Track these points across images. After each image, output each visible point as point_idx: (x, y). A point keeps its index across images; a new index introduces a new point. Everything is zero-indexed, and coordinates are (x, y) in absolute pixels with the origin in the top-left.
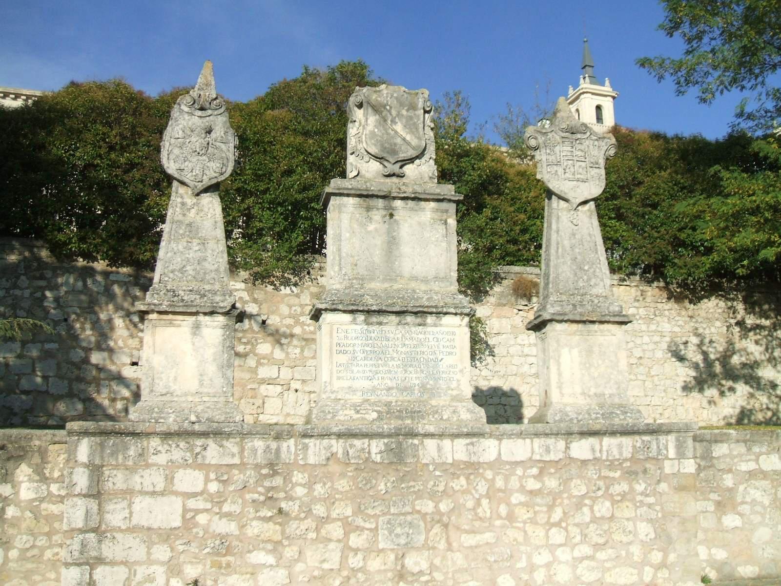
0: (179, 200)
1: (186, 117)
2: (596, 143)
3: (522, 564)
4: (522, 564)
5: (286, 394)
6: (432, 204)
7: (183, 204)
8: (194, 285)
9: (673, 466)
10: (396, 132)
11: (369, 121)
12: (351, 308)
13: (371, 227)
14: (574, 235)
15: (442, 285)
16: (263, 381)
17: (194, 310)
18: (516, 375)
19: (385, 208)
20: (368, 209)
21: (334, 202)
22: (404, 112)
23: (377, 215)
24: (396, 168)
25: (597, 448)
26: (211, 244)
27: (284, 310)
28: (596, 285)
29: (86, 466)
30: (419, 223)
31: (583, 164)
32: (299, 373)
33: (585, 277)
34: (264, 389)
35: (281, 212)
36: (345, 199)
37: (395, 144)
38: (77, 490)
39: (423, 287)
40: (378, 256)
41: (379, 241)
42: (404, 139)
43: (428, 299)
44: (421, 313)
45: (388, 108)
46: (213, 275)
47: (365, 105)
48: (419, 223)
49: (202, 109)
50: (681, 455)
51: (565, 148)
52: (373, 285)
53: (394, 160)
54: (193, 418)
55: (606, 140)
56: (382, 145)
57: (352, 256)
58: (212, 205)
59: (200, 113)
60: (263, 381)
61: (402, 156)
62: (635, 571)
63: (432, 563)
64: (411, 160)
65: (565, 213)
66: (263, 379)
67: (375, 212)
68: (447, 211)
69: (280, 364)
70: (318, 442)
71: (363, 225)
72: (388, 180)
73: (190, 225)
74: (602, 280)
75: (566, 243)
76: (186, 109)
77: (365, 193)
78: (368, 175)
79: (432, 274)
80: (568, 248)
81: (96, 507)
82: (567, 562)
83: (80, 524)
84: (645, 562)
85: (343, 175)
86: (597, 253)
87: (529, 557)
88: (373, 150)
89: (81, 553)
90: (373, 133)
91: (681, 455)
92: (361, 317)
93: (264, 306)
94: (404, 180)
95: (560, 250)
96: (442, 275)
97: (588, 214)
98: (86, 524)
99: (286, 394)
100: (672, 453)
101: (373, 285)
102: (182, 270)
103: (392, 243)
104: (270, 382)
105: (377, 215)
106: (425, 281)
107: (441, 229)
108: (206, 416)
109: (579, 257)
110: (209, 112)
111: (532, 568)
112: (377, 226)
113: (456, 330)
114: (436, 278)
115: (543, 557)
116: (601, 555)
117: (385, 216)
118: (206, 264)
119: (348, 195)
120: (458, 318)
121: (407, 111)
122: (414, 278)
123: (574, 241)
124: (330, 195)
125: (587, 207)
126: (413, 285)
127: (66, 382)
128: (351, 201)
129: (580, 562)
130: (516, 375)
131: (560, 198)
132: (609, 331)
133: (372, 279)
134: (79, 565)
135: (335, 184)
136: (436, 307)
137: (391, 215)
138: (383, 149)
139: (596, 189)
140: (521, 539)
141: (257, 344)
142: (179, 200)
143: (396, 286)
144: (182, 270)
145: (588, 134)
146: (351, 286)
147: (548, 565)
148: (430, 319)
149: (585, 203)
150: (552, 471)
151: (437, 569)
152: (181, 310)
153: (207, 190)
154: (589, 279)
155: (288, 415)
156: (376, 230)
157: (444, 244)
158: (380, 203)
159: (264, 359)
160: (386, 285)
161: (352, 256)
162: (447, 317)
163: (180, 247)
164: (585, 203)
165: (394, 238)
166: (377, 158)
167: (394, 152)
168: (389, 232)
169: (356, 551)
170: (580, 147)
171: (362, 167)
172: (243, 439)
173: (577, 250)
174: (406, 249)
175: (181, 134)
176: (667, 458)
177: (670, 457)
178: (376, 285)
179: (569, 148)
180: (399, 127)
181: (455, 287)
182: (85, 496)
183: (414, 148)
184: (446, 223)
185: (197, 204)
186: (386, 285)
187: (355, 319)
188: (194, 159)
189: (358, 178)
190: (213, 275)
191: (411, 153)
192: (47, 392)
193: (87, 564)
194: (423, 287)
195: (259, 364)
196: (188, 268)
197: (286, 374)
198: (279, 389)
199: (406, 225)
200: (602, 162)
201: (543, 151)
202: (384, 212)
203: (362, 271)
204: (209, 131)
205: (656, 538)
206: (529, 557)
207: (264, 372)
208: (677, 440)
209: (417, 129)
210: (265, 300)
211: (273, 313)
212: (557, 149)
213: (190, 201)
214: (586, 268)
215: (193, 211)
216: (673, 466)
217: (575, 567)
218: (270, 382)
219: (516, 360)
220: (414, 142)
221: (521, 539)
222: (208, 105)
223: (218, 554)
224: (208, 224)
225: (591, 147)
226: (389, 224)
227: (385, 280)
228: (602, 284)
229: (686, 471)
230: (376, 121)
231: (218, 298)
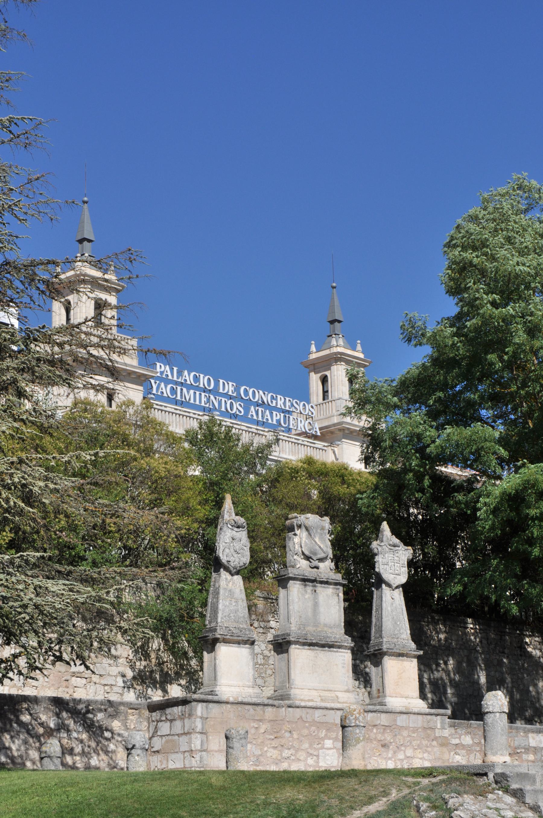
7: (226, 579)
13: (307, 596)
14: (392, 604)
20: (305, 585)
22: (319, 531)
26: (240, 603)
29: (201, 718)
38: (198, 730)
41: (310, 604)
42: (320, 547)
44: (330, 646)
46: (242, 619)
47: (303, 526)
59: (236, 529)
71: (302, 595)
72: (313, 570)
73: (230, 591)
75: (389, 608)
81: (205, 739)
88: (307, 553)
98: (201, 748)
100: (439, 726)
102: (229, 616)
103: (316, 605)
106: (331, 628)
122: (325, 625)
138: (311, 552)
139: (403, 579)
154: (400, 630)
156: (309, 598)
157: (338, 607)
165: (316, 603)
181: (343, 631)
184: (338, 596)
190: (242, 619)
196: (232, 615)
200: (406, 563)
208: (442, 719)
212: (387, 555)
215: (231, 583)
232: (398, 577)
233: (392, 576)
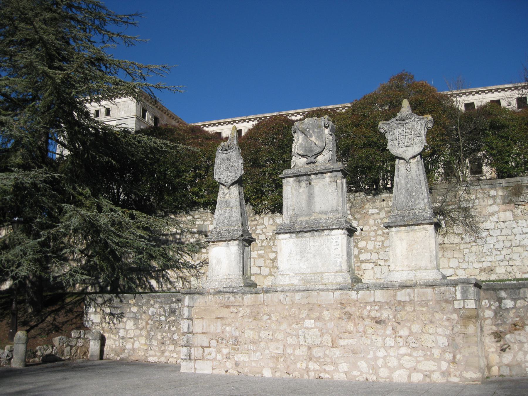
0: (222, 191)
1: (221, 155)
2: (419, 122)
3: (371, 356)
4: (371, 356)
5: (375, 268)
6: (329, 174)
7: (224, 193)
8: (227, 228)
9: (459, 304)
10: (312, 141)
11: (300, 139)
12: (287, 231)
13: (301, 190)
14: (407, 177)
15: (334, 214)
16: (362, 262)
17: (224, 239)
18: (518, 246)
19: (307, 180)
20: (299, 182)
21: (284, 181)
22: (316, 130)
23: (304, 184)
24: (312, 159)
25: (412, 295)
26: (235, 209)
27: (371, 222)
28: (419, 203)
29: (188, 307)
30: (323, 185)
31: (410, 136)
32: (382, 256)
33: (413, 200)
34: (364, 266)
35: (262, 191)
36: (289, 179)
37: (311, 147)
38: (185, 317)
39: (325, 217)
40: (304, 204)
41: (304, 197)
42: (315, 144)
43: (325, 223)
45: (308, 130)
46: (235, 223)
48: (323, 185)
49: (226, 150)
50: (465, 298)
51: (400, 130)
52: (301, 219)
53: (311, 155)
54: (225, 286)
55: (424, 120)
56: (305, 149)
57: (292, 206)
58: (235, 191)
59: (225, 152)
60: (362, 262)
61: (315, 152)
62: (436, 364)
63: (325, 353)
64: (320, 153)
65: (402, 165)
66: (363, 260)
67: (303, 183)
68: (336, 176)
69: (371, 251)
70: (273, 294)
71: (297, 190)
72: (309, 166)
73: (226, 202)
74: (423, 200)
75: (403, 182)
76: (220, 151)
77: (296, 175)
78: (300, 165)
79: (330, 209)
80: (404, 185)
81: (191, 324)
82: (395, 356)
83: (186, 330)
84: (441, 359)
85: (289, 167)
86: (420, 185)
87: (374, 353)
88: (301, 152)
89: (187, 342)
90: (301, 144)
91: (465, 298)
92: (294, 235)
93: (361, 222)
94: (316, 164)
95: (399, 187)
96: (335, 209)
97: (416, 163)
98: (188, 330)
99: (375, 268)
100: (459, 296)
101: (301, 219)
102: (223, 222)
103: (311, 196)
104: (366, 261)
105: (304, 184)
106: (326, 213)
107: (334, 186)
108: (229, 284)
109: (410, 189)
110: (229, 151)
111: (376, 358)
112: (304, 189)
113: (340, 237)
114: (332, 211)
115: (381, 353)
116: (415, 354)
117: (307, 184)
118: (232, 218)
119: (290, 177)
120: (340, 231)
121: (317, 129)
122: (321, 213)
123: (407, 180)
124: (282, 178)
125: (416, 159)
126: (320, 216)
127: (268, 269)
128: (291, 179)
129: (402, 357)
130: (518, 246)
131: (400, 158)
132: (424, 229)
133: (301, 215)
134: (186, 347)
135: (286, 171)
136: (327, 226)
137: (310, 184)
138: (306, 151)
140: (369, 343)
141: (358, 242)
142: (222, 191)
143: (312, 218)
144: (223, 222)
145: (413, 118)
146: (292, 220)
147: (384, 358)
148: (326, 232)
149: (414, 157)
150: (387, 307)
151: (328, 356)
152: (220, 240)
153: (232, 184)
154: (415, 200)
155: (377, 278)
156: (303, 191)
157: (336, 193)
158: (304, 178)
159: (362, 249)
160: (307, 218)
161: (292, 206)
162: (334, 231)
163: (223, 212)
164: (414, 157)
165: (311, 194)
166: (303, 156)
167: (311, 151)
168: (309, 192)
169: (290, 345)
170: (408, 127)
171: (298, 162)
172: (243, 294)
173: (409, 185)
174: (317, 199)
175: (220, 163)
176: (456, 299)
177: (457, 298)
178: (303, 219)
179: (402, 129)
180: (313, 139)
182: (188, 319)
183: (320, 148)
185: (229, 192)
186: (307, 218)
187: (291, 236)
188: (224, 173)
189: (295, 168)
190: (235, 223)
191: (319, 150)
192: (260, 274)
193: (189, 346)
194: (325, 217)
195: (360, 252)
196: (225, 221)
197: (375, 256)
198: (372, 265)
199: (317, 187)
200: (423, 132)
201: (388, 133)
202: (306, 182)
203: (296, 212)
204: (229, 160)
205: (448, 345)
206: (374, 353)
207: (363, 257)
208: (463, 289)
209: (322, 137)
210: (361, 218)
211: (365, 225)
212: (395, 131)
213: (226, 191)
214: (414, 194)
215: (228, 195)
216: (459, 304)
217: (399, 360)
218: (366, 261)
219: (518, 237)
220: (320, 144)
221: (369, 343)
222: (227, 148)
223: (234, 344)
224: (233, 200)
225: (415, 126)
226: (309, 187)
227: (307, 215)
228: (423, 202)
229: (469, 307)
230: (303, 137)
231: (235, 233)
232: (409, 149)
233: (402, 149)
